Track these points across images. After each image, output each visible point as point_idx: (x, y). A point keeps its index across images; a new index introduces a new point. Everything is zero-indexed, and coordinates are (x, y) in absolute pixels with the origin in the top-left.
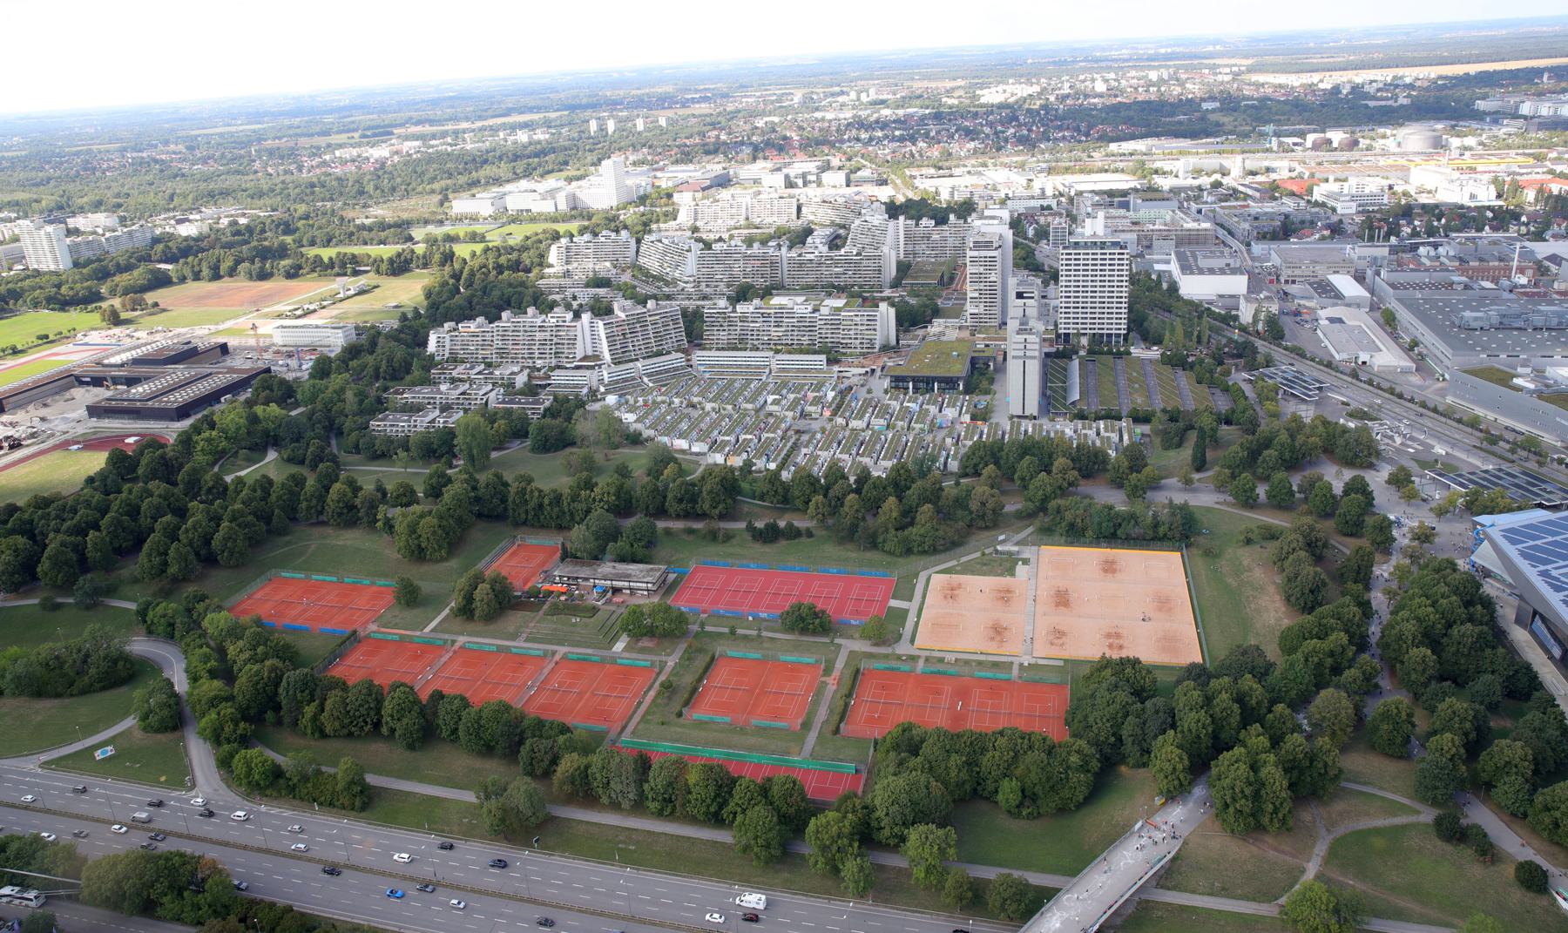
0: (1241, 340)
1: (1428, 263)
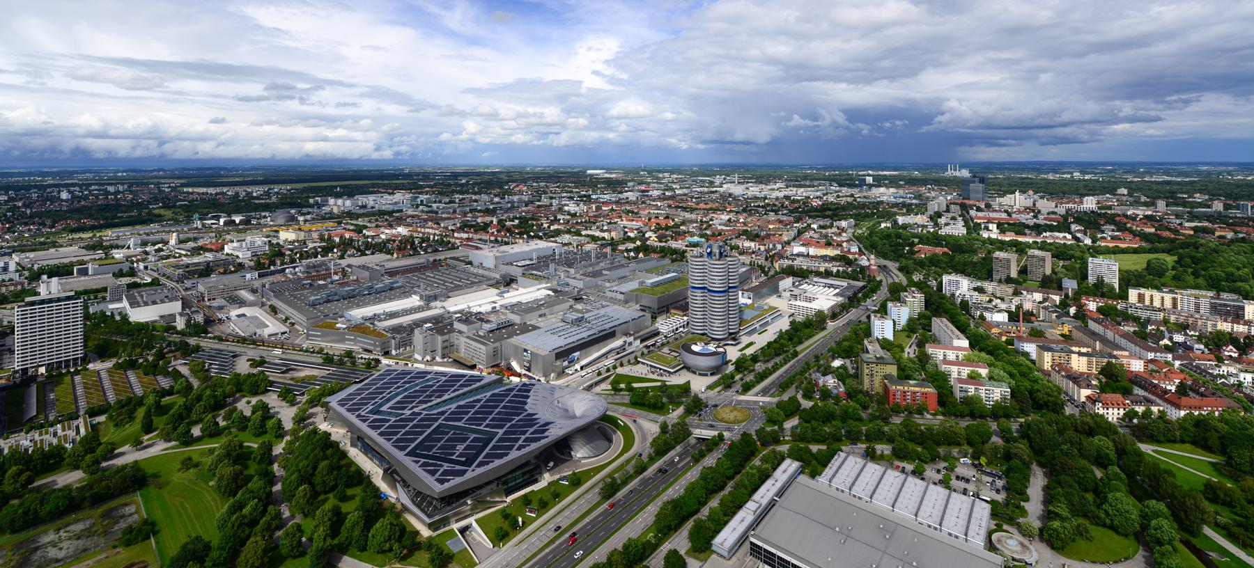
0: (178, 340)
1: (291, 277)
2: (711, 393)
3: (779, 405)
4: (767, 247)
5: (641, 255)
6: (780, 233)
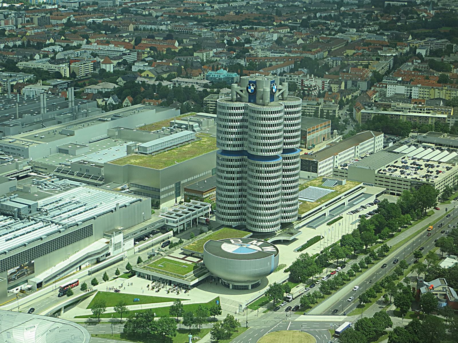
2: (252, 314)
3: (360, 325)
4: (343, 88)
5: (127, 101)
6: (365, 63)
